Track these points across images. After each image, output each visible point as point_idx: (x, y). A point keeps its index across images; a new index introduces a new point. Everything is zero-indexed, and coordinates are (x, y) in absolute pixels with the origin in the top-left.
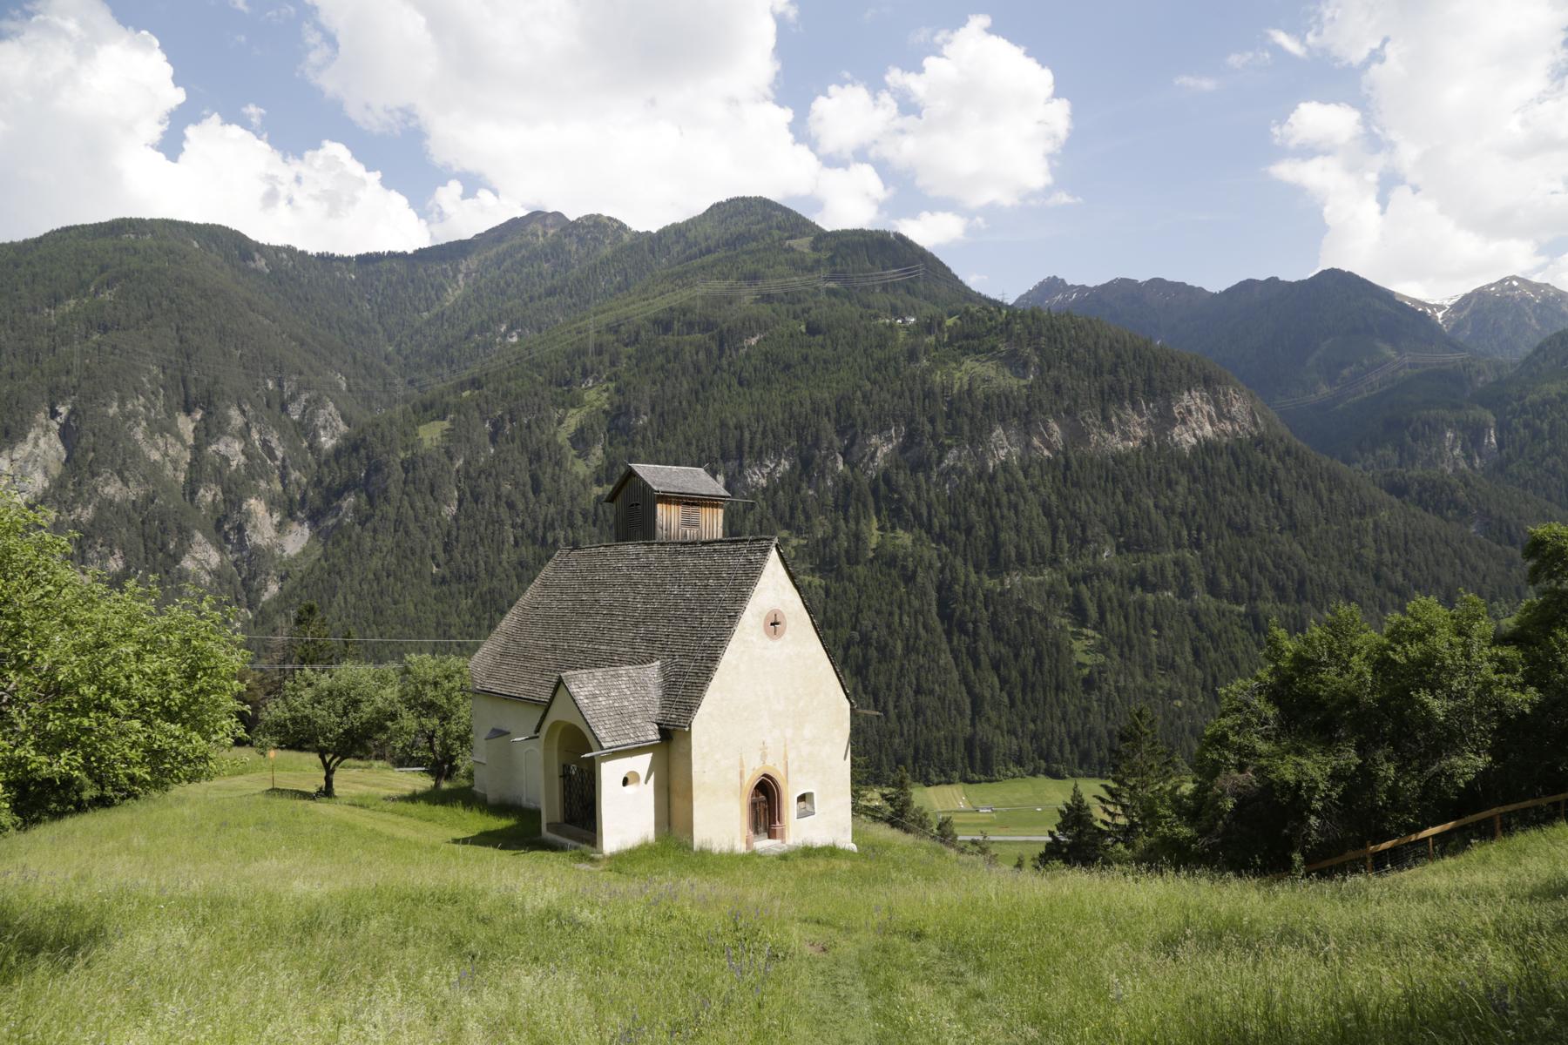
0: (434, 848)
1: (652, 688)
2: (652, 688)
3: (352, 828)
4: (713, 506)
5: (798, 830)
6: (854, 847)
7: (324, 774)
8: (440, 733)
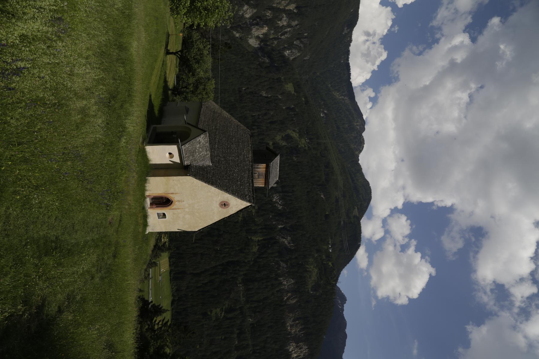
0: (148, 88)
1: (202, 162)
2: (202, 162)
3: (156, 61)
5: (153, 214)
6: (147, 233)
7: (174, 52)
8: (187, 90)
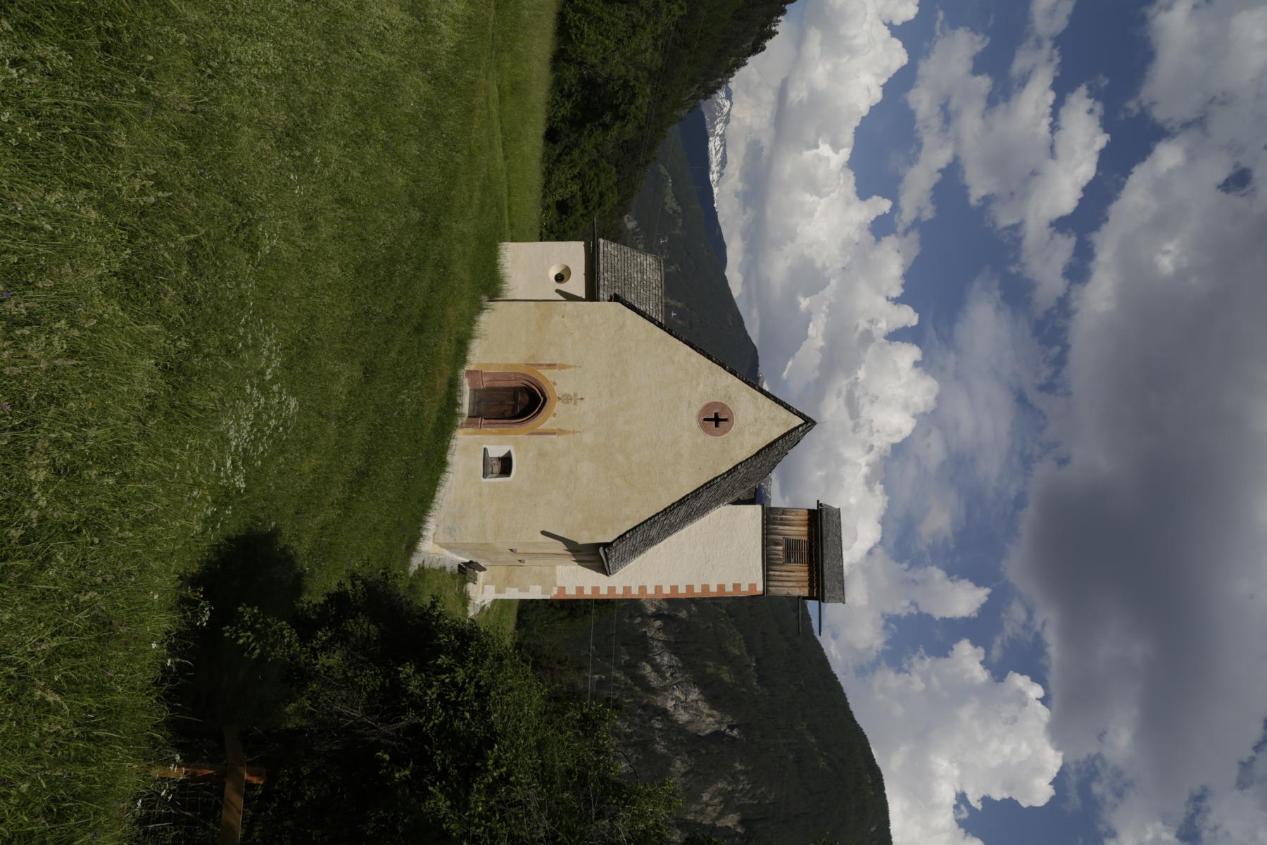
4: (811, 581)
5: (469, 447)
